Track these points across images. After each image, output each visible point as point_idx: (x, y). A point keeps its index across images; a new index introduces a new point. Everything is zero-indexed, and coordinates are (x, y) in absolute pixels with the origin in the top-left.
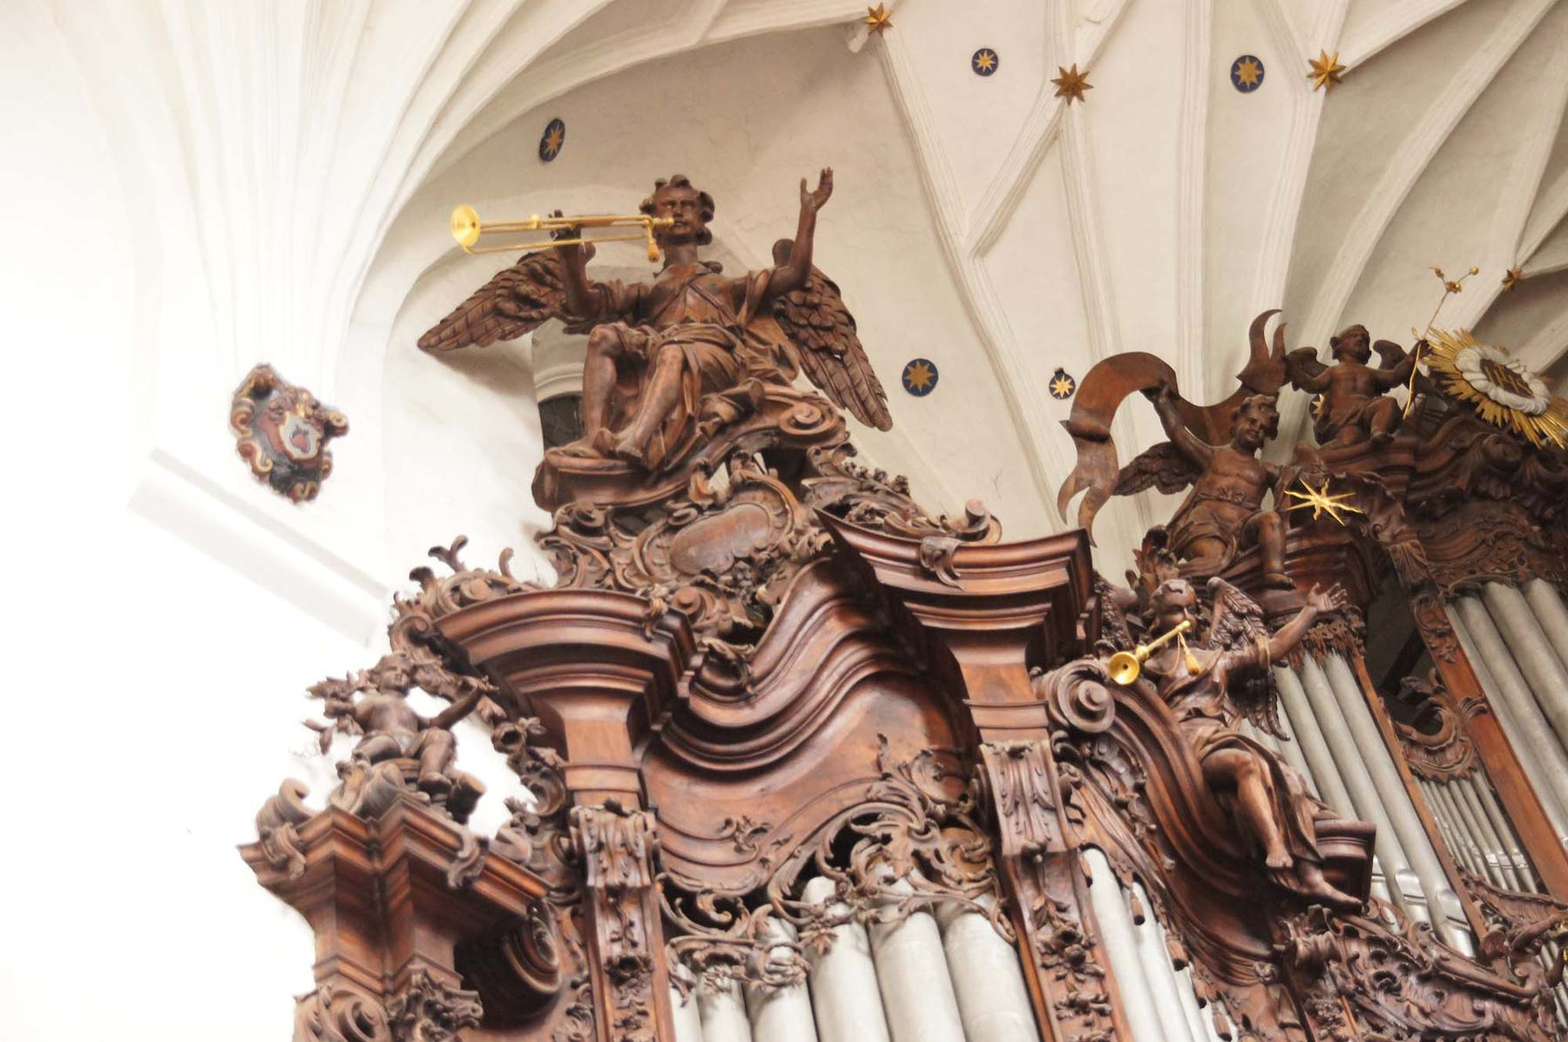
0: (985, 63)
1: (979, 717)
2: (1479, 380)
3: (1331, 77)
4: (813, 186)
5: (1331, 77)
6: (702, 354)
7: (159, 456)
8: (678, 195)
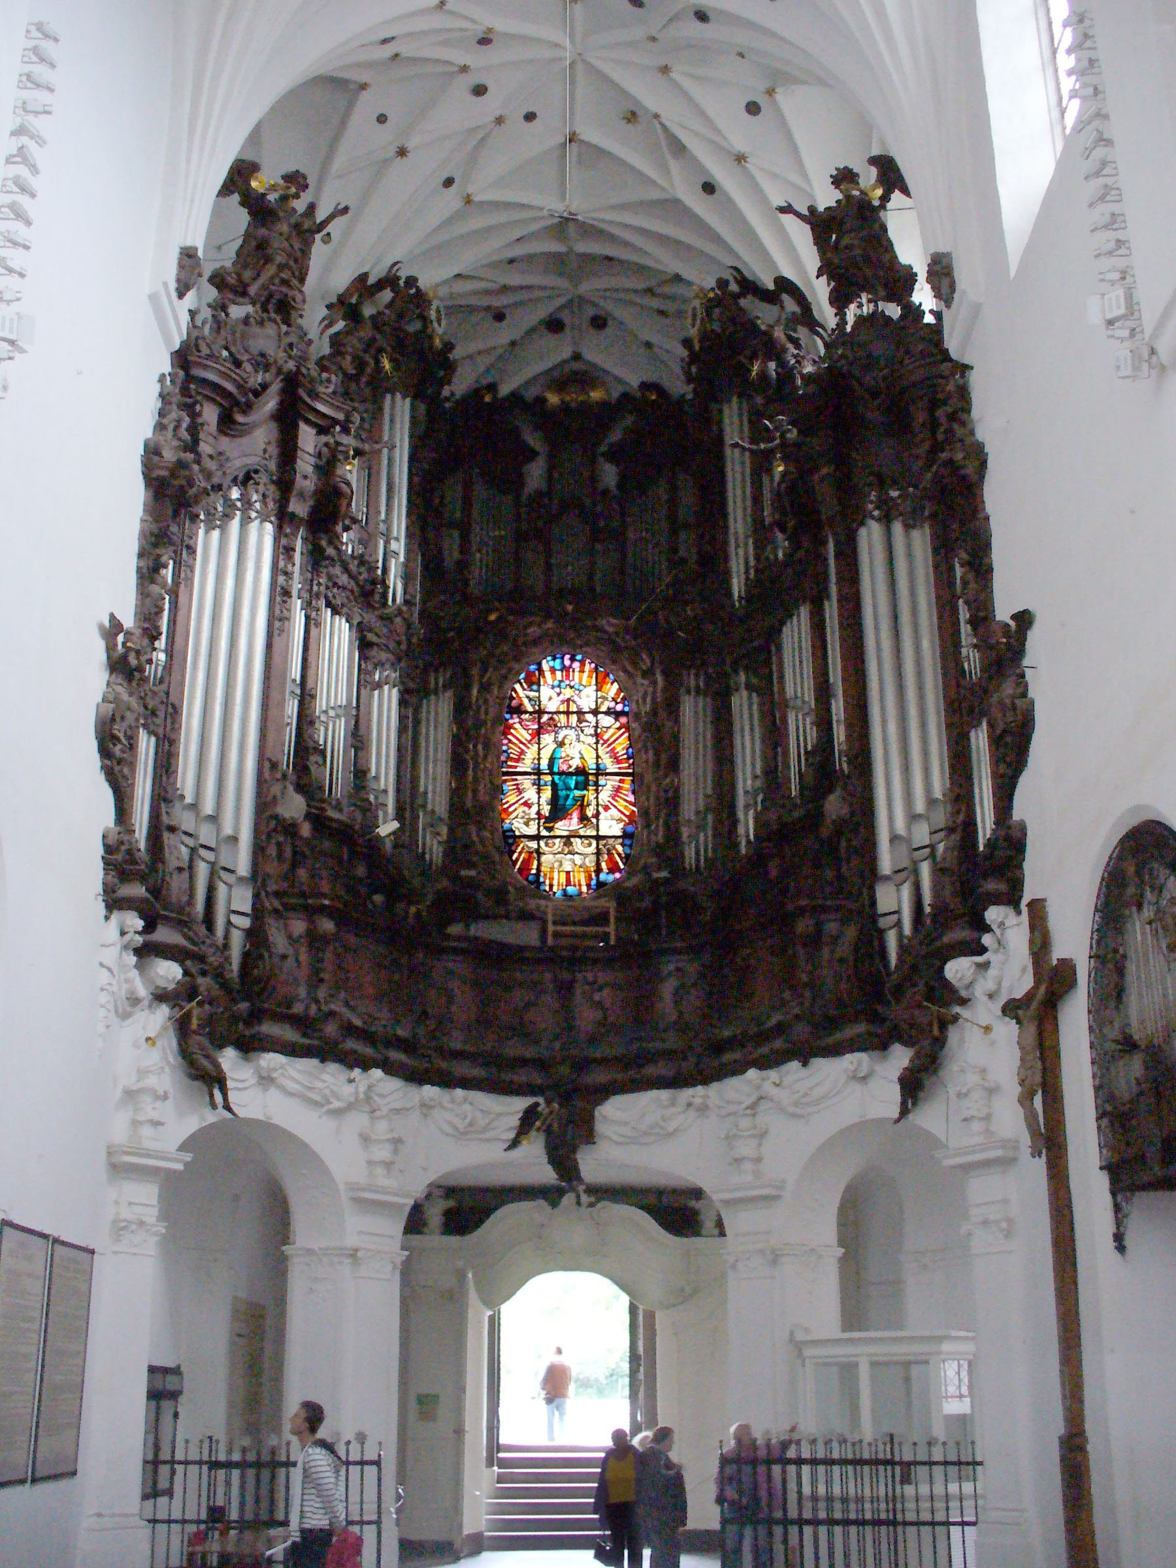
0: (382, 119)
1: (299, 453)
3: (468, 200)
4: (340, 207)
5: (468, 200)
7: (165, 285)
8: (301, 181)
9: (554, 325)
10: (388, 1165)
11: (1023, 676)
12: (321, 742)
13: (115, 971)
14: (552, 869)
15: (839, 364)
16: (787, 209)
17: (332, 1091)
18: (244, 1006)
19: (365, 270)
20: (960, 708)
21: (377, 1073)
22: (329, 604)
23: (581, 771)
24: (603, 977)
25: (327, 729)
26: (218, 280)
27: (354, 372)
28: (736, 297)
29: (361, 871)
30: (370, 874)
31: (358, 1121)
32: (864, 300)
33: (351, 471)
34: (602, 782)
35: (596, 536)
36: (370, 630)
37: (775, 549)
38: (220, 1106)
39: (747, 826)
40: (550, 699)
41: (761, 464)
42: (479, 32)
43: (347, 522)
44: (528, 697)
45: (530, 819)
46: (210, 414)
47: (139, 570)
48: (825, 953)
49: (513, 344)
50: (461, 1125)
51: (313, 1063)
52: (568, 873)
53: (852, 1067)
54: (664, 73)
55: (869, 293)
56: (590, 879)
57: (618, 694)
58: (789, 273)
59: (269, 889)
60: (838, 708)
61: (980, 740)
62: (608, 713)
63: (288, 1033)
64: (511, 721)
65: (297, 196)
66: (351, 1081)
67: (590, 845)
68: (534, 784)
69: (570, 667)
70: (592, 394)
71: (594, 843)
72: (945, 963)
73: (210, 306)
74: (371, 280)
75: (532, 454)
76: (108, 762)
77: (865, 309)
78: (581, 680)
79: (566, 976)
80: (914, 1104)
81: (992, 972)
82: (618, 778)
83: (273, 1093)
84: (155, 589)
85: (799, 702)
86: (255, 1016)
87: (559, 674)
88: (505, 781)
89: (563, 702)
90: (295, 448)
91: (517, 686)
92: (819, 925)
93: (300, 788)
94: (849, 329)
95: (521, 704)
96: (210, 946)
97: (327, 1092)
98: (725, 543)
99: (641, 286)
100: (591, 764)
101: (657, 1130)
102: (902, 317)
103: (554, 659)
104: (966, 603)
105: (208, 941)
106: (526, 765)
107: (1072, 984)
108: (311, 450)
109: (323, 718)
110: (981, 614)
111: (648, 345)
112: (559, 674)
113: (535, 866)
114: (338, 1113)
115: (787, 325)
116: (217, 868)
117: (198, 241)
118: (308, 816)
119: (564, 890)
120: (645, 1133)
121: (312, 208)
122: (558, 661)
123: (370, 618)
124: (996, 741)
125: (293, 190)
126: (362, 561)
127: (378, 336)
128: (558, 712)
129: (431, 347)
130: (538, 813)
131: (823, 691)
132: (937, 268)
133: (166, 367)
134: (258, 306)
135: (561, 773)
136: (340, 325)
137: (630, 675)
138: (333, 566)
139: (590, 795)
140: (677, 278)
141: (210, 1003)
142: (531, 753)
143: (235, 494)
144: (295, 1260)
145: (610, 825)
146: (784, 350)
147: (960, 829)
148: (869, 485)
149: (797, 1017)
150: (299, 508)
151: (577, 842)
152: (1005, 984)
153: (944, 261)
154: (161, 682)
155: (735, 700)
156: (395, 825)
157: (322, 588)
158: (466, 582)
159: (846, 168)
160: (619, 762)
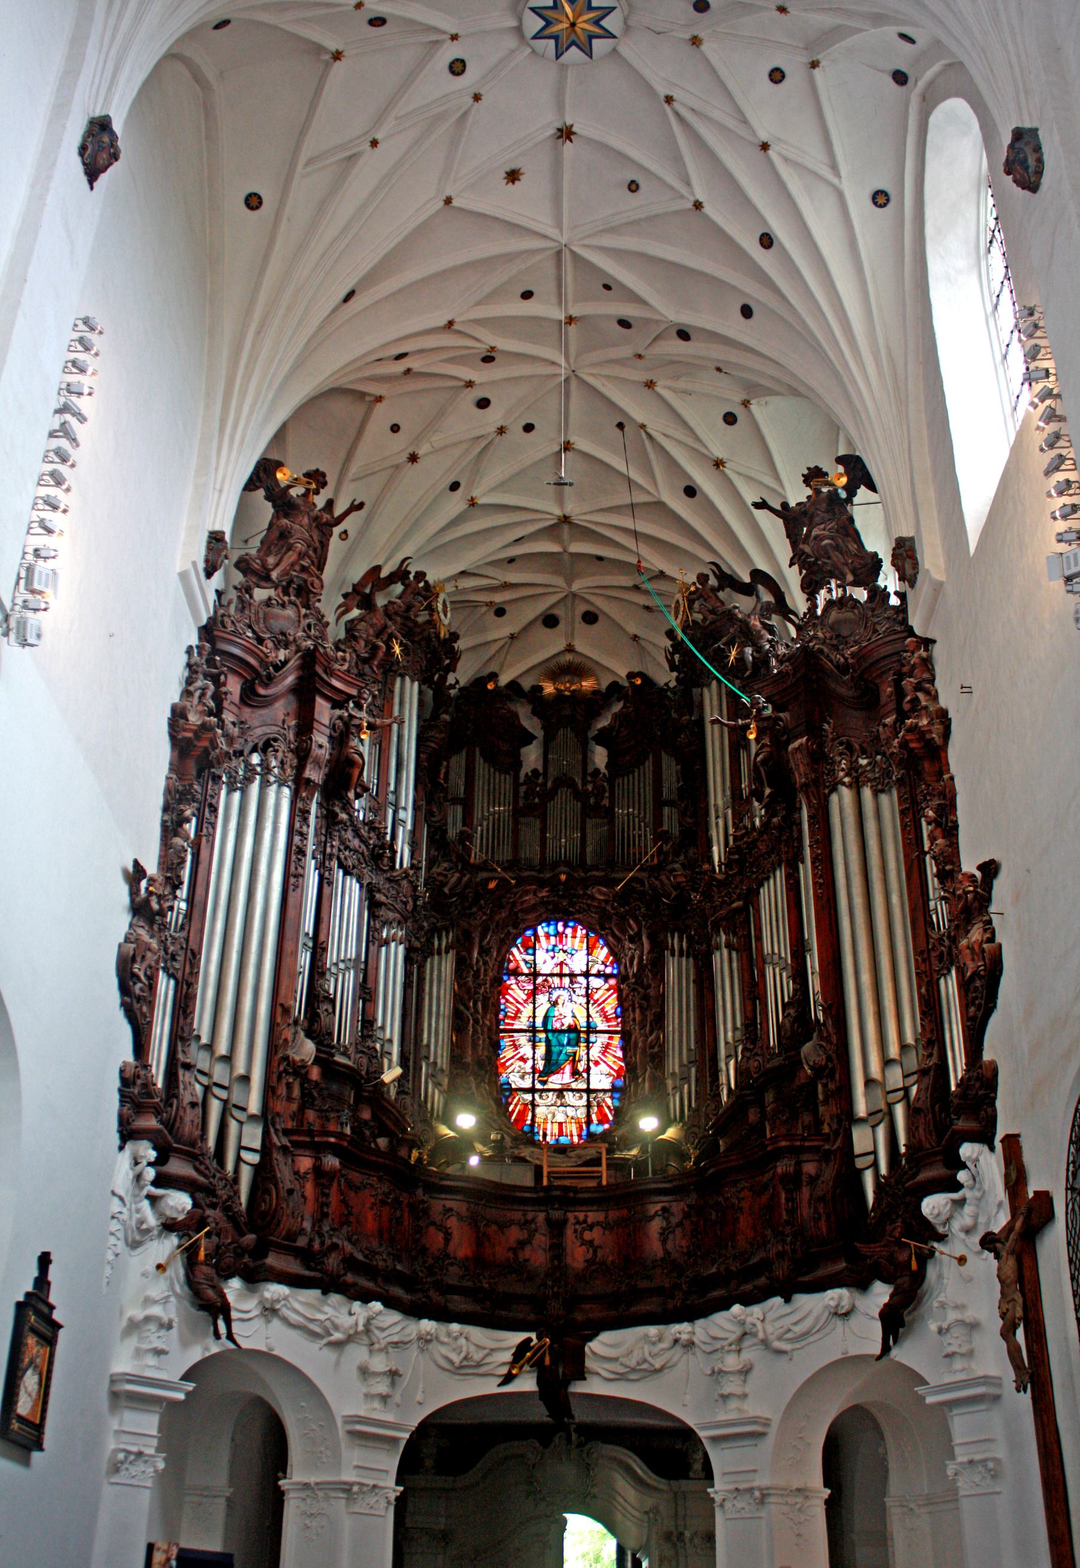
0: (395, 428)
1: (316, 725)
2: (440, 607)
3: (472, 503)
4: (356, 503)
5: (472, 503)
6: (304, 549)
8: (321, 479)
9: (550, 621)
10: (384, 1398)
11: (990, 922)
12: (332, 991)
13: (127, 1199)
14: (546, 1119)
15: (811, 644)
16: (762, 505)
17: (333, 1323)
18: (250, 1238)
19: (380, 563)
20: (929, 957)
21: (377, 1306)
22: (341, 865)
23: (573, 1029)
24: (592, 1217)
25: (336, 980)
26: (243, 565)
27: (366, 655)
28: (714, 590)
29: (366, 1115)
30: (374, 1114)
31: (358, 1354)
32: (833, 586)
33: (364, 745)
34: (592, 1038)
35: (589, 811)
36: (379, 891)
37: (752, 819)
38: (224, 1337)
39: (729, 1073)
40: (545, 962)
41: (738, 742)
42: (482, 349)
43: (358, 790)
44: (524, 960)
45: (525, 1073)
46: (233, 686)
47: (164, 824)
48: (806, 1191)
49: (512, 637)
50: (456, 1359)
51: (315, 1294)
52: (560, 1124)
53: (833, 1303)
54: (649, 387)
55: (837, 578)
56: (581, 1129)
57: (607, 957)
58: (762, 566)
59: (278, 1127)
60: (813, 962)
61: (950, 987)
62: (598, 975)
63: (294, 1266)
64: (508, 982)
65: (317, 492)
66: (350, 1314)
67: (581, 1098)
68: (529, 1041)
69: (563, 932)
70: (584, 684)
71: (585, 1096)
72: (921, 1200)
73: (235, 588)
74: (384, 573)
75: (529, 738)
76: (127, 999)
77: (834, 593)
78: (573, 945)
79: (556, 1214)
80: (895, 1342)
81: (968, 1209)
82: (607, 1036)
83: (276, 1323)
84: (178, 841)
85: (776, 957)
86: (260, 1250)
87: (553, 939)
88: (503, 1037)
89: (556, 965)
90: (312, 719)
91: (514, 950)
92: (799, 1164)
93: (309, 1034)
94: (819, 612)
95: (518, 967)
96: (221, 1179)
97: (328, 1324)
98: (707, 813)
99: (630, 583)
100: (582, 1022)
101: (645, 1366)
102: (871, 598)
103: (549, 925)
104: (933, 858)
105: (218, 1175)
106: (522, 1023)
107: (1049, 1216)
108: (326, 722)
109: (334, 970)
110: (948, 867)
111: (636, 636)
112: (553, 939)
113: (529, 1117)
114: (338, 1345)
115: (762, 616)
116: (230, 1106)
117: (226, 526)
118: (317, 1060)
119: (557, 1140)
120: (633, 1370)
121: (330, 504)
122: (552, 928)
123: (378, 880)
124: (964, 986)
125: (314, 486)
126: (371, 825)
127: (390, 623)
128: (552, 975)
129: (438, 635)
130: (533, 1067)
131: (799, 948)
132: (898, 551)
133: (193, 639)
134: (280, 589)
135: (555, 1031)
136: (356, 613)
137: (618, 940)
138: (346, 830)
139: (582, 1051)
140: (662, 575)
141: (218, 1235)
142: (527, 1011)
143: (255, 759)
144: (292, 1495)
145: (600, 1079)
146: (761, 637)
147: (932, 1073)
148: (841, 754)
149: (780, 1255)
150: (314, 774)
151: (569, 1097)
152: (982, 1220)
153: (907, 543)
154: (182, 928)
155: (716, 958)
156: (398, 1071)
157: (335, 851)
158: (468, 850)
159: (816, 467)
160: (608, 1020)
